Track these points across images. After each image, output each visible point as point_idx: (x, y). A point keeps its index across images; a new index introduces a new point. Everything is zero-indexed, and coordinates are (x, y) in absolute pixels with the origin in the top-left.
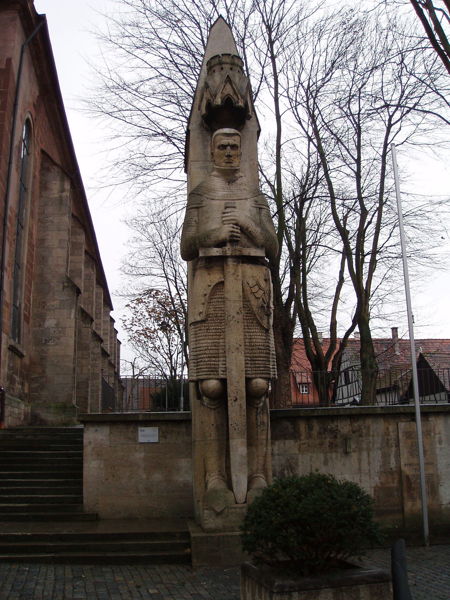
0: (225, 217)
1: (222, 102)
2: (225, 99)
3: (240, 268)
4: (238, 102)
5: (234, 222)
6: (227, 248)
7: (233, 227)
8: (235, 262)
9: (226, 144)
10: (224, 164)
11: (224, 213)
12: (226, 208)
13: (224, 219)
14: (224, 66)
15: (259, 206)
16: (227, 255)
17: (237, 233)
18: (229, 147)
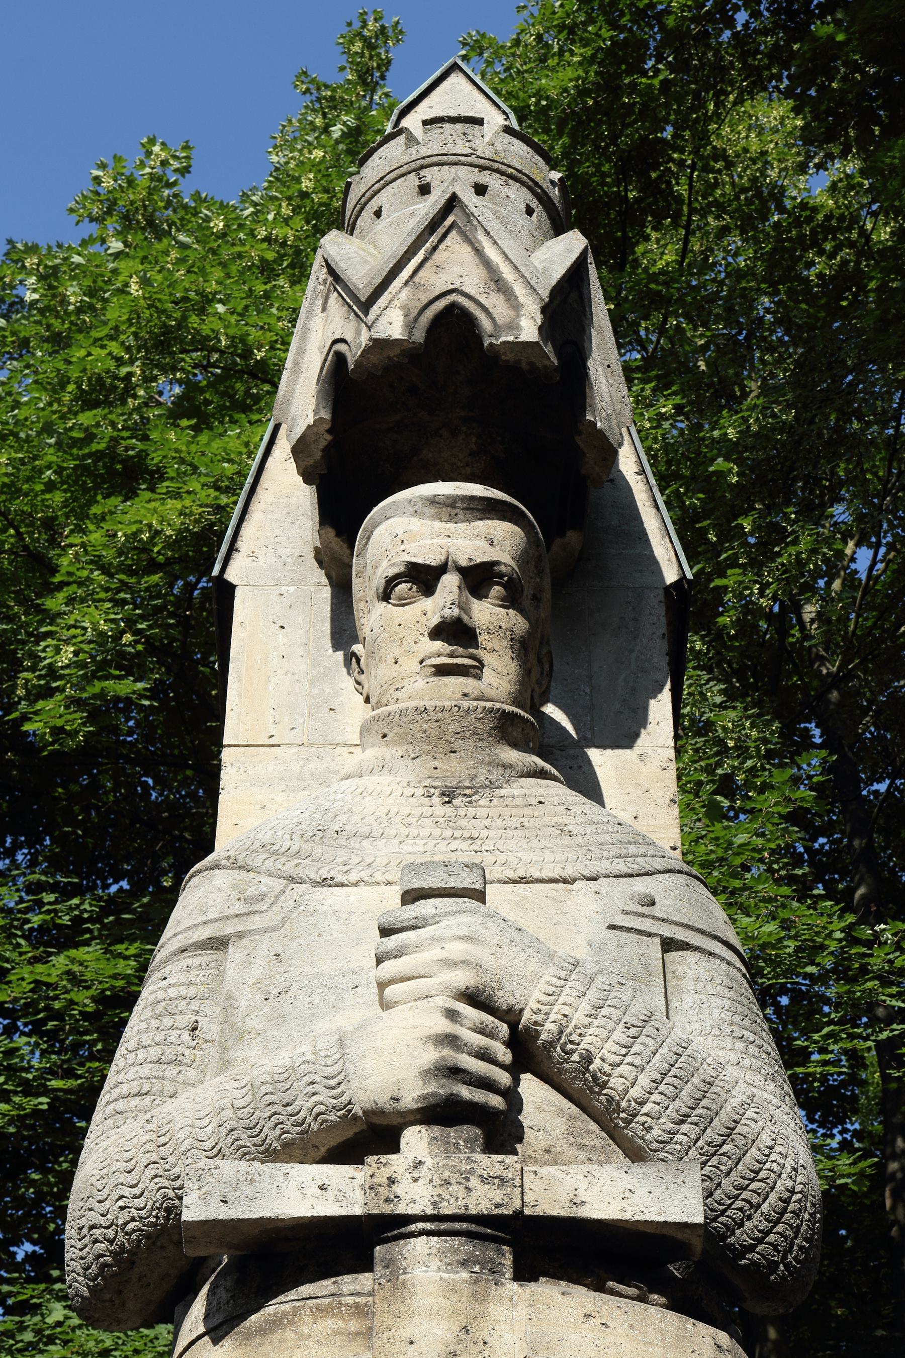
0: (398, 954)
1: (410, 326)
2: (430, 313)
3: (497, 1310)
4: (513, 326)
5: (463, 979)
6: (397, 1163)
7: (452, 1015)
8: (464, 1264)
9: (433, 559)
10: (421, 683)
11: (386, 932)
12: (411, 897)
13: (390, 968)
14: (429, 175)
15: (667, 931)
16: (402, 1209)
17: (484, 1056)
18: (450, 582)
